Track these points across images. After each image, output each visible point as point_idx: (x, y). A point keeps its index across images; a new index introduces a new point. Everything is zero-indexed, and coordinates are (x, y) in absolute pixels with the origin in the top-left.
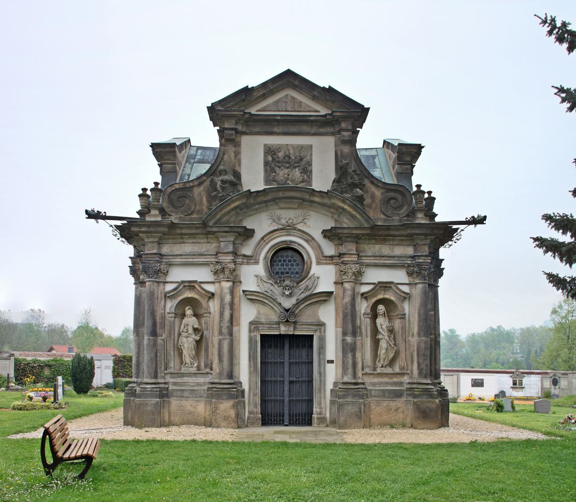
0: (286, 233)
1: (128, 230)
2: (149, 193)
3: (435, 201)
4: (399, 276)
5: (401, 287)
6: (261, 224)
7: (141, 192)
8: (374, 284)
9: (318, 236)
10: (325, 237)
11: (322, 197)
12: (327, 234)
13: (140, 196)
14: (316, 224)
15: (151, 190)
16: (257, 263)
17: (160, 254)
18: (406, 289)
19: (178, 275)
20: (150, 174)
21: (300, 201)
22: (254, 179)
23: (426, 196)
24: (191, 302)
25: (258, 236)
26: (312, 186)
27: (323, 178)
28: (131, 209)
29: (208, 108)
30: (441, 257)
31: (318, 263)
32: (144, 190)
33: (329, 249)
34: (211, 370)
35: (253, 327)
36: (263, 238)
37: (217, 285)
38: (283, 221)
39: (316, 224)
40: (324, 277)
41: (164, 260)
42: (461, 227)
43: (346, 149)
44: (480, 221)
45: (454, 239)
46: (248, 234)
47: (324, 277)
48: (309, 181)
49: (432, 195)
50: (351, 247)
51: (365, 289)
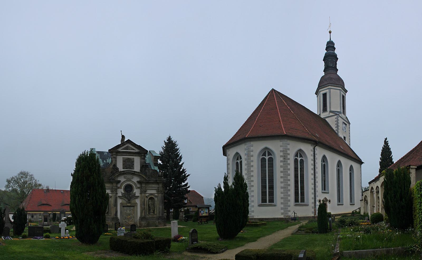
5: (155, 194)
6: (122, 179)
10: (138, 182)
12: (138, 182)
14: (136, 179)
16: (121, 189)
18: (156, 195)
22: (121, 168)
25: (121, 182)
26: (134, 169)
27: (137, 168)
31: (136, 189)
33: (139, 186)
34: (111, 214)
35: (121, 204)
36: (123, 182)
37: (112, 194)
39: (136, 179)
43: (143, 161)
47: (137, 192)
50: (143, 185)
51: (147, 195)
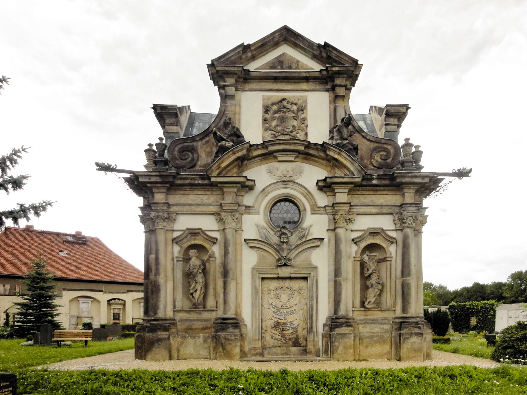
0: (284, 186)
1: (136, 183)
2: (154, 148)
3: (423, 155)
4: (386, 223)
5: (387, 232)
6: (260, 174)
7: (148, 147)
8: (364, 230)
9: (312, 186)
11: (317, 149)
13: (146, 151)
15: (156, 145)
17: (168, 203)
19: (184, 223)
20: (154, 133)
21: (297, 154)
23: (414, 150)
24: (195, 245)
28: (140, 164)
29: (208, 66)
30: (424, 206)
32: (150, 145)
33: (322, 199)
38: (279, 173)
40: (316, 224)
41: (172, 210)
42: (447, 179)
44: (462, 174)
45: (441, 191)
46: (247, 187)
48: (307, 138)
49: (420, 149)
